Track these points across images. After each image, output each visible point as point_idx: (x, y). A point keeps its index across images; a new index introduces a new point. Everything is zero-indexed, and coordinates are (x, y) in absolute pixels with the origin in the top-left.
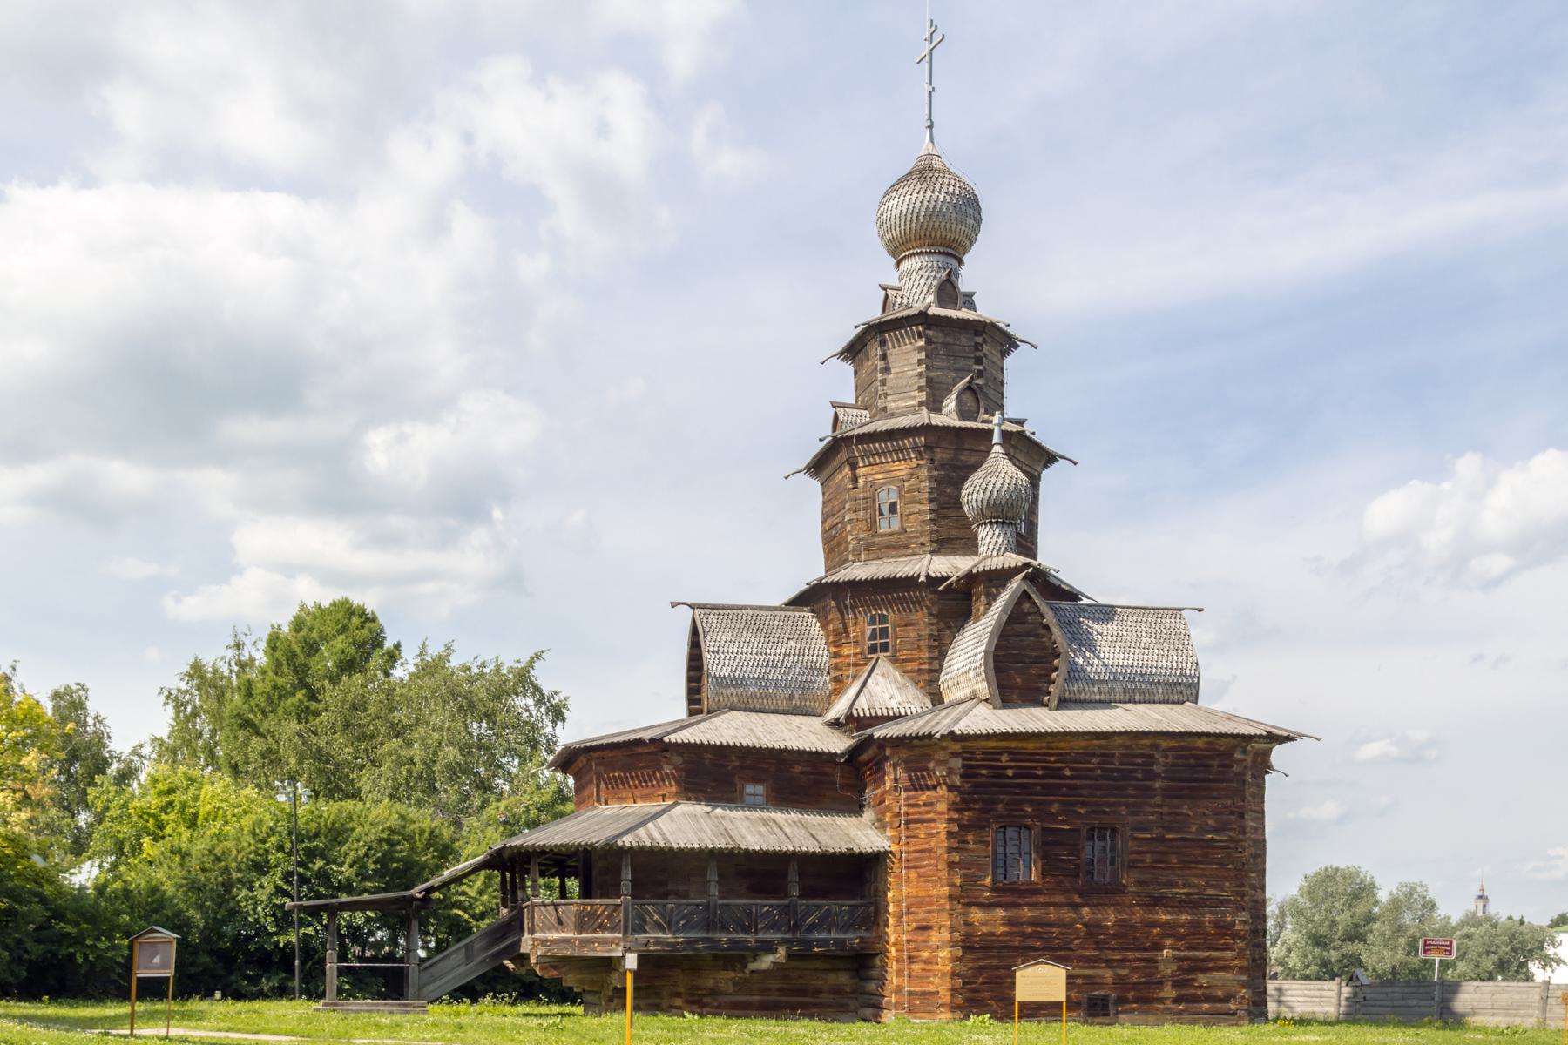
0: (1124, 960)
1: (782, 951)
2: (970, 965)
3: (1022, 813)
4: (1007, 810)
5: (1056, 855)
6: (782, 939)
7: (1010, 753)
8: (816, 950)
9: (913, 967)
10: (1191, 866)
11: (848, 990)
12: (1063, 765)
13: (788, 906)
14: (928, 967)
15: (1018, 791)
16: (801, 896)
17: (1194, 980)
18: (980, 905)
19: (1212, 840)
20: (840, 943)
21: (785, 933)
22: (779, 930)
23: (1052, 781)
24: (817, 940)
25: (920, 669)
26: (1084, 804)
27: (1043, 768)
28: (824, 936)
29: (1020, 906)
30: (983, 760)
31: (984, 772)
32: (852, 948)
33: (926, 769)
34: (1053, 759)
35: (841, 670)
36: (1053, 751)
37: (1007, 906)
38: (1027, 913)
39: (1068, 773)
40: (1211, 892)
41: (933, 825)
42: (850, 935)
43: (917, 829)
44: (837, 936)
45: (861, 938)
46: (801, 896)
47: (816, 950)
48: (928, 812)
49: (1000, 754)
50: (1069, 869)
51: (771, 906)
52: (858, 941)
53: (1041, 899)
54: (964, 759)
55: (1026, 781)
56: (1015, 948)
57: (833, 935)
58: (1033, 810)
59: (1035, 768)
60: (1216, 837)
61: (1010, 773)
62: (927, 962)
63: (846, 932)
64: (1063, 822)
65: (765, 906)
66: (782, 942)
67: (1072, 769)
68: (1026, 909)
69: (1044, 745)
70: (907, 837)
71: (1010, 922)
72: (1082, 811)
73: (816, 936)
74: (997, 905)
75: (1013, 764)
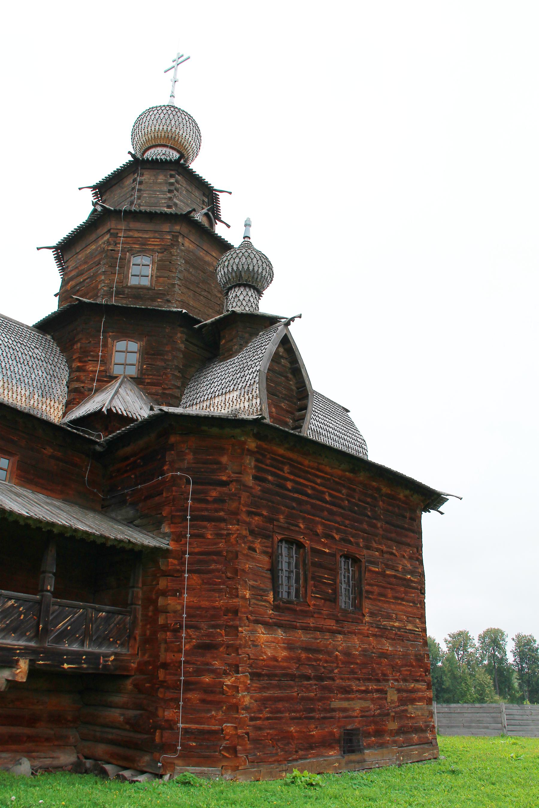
0: (366, 691)
1: (23, 665)
2: (257, 695)
3: (297, 529)
4: (287, 523)
5: (320, 577)
6: (26, 648)
7: (291, 465)
8: (66, 666)
9: (189, 696)
10: (399, 602)
11: (69, 718)
12: (325, 490)
13: (40, 603)
14: (210, 698)
15: (294, 505)
16: (56, 594)
17: (406, 710)
18: (265, 624)
19: (410, 580)
20: (93, 658)
21: (29, 640)
22: (22, 635)
23: (318, 502)
24: (68, 653)
25: (164, 393)
26: (338, 531)
27: (313, 488)
28: (75, 647)
29: (295, 628)
30: (272, 466)
31: (270, 478)
32: (105, 666)
33: (219, 463)
34: (319, 481)
35: (83, 382)
36: (320, 474)
37: (287, 627)
38: (301, 637)
39: (328, 498)
40: (410, 627)
41: (223, 525)
42: (103, 650)
43: (205, 527)
44: (90, 650)
45: (116, 654)
46: (56, 594)
47: (66, 666)
48: (217, 511)
49: (283, 463)
50: (328, 593)
51: (17, 599)
52: (113, 657)
53: (311, 622)
54: (257, 460)
55: (300, 496)
56: (293, 677)
57: (86, 649)
58: (305, 528)
59: (307, 486)
60: (412, 578)
61: (289, 485)
62: (208, 690)
63: (100, 645)
64: (325, 545)
65: (10, 599)
66: (26, 651)
67: (330, 495)
68: (300, 632)
69: (316, 465)
70: (192, 536)
71: (290, 647)
72: (337, 537)
73: (66, 646)
74: (279, 625)
75: (292, 477)
